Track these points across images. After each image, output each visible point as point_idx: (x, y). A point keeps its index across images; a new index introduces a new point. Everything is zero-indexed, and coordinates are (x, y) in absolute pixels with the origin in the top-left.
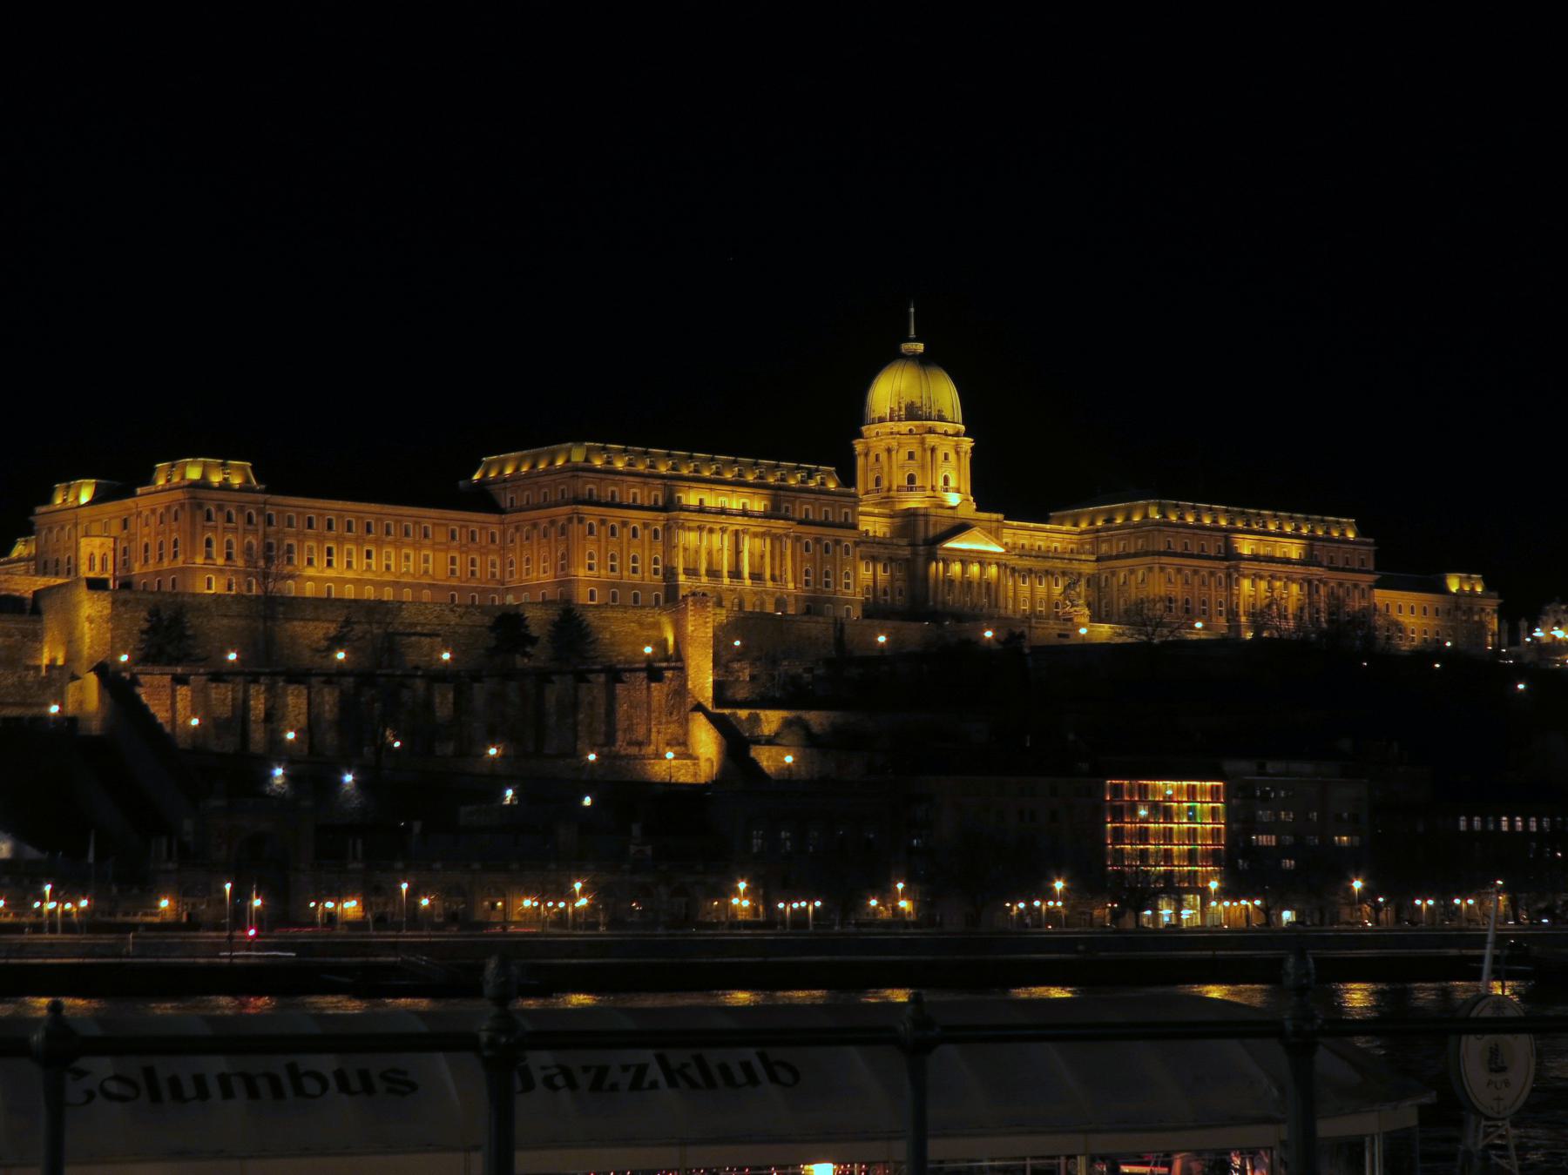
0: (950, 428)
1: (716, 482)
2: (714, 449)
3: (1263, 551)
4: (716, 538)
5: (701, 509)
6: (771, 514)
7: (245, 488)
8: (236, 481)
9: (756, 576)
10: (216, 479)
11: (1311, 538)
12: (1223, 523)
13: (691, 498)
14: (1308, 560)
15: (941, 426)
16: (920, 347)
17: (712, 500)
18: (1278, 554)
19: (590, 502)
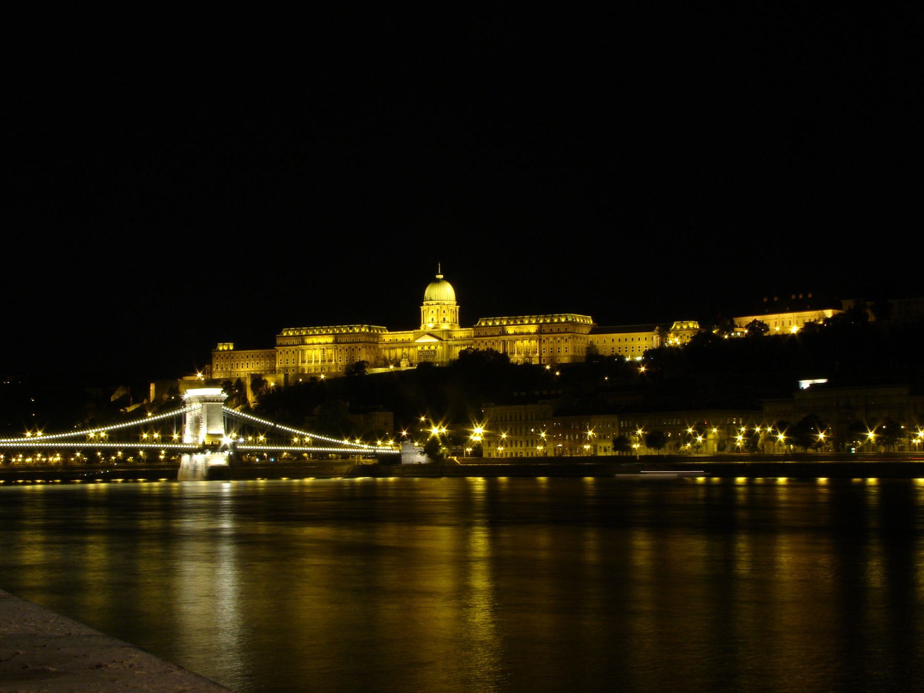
0: (434, 302)
1: (321, 334)
2: (321, 325)
3: (518, 331)
4: (317, 352)
5: (313, 344)
6: (336, 342)
7: (229, 350)
8: (226, 348)
9: (317, 361)
10: (221, 348)
11: (545, 323)
12: (505, 323)
13: (309, 340)
14: (540, 332)
15: (431, 303)
16: (441, 276)
17: (315, 340)
18: (525, 331)
19: (281, 345)
